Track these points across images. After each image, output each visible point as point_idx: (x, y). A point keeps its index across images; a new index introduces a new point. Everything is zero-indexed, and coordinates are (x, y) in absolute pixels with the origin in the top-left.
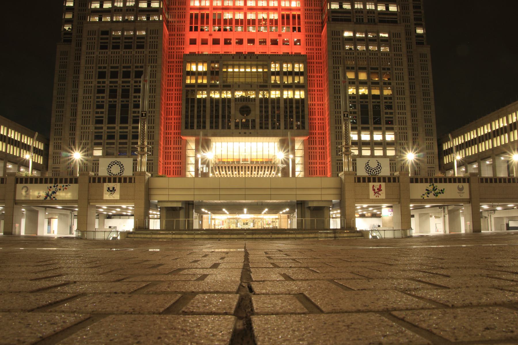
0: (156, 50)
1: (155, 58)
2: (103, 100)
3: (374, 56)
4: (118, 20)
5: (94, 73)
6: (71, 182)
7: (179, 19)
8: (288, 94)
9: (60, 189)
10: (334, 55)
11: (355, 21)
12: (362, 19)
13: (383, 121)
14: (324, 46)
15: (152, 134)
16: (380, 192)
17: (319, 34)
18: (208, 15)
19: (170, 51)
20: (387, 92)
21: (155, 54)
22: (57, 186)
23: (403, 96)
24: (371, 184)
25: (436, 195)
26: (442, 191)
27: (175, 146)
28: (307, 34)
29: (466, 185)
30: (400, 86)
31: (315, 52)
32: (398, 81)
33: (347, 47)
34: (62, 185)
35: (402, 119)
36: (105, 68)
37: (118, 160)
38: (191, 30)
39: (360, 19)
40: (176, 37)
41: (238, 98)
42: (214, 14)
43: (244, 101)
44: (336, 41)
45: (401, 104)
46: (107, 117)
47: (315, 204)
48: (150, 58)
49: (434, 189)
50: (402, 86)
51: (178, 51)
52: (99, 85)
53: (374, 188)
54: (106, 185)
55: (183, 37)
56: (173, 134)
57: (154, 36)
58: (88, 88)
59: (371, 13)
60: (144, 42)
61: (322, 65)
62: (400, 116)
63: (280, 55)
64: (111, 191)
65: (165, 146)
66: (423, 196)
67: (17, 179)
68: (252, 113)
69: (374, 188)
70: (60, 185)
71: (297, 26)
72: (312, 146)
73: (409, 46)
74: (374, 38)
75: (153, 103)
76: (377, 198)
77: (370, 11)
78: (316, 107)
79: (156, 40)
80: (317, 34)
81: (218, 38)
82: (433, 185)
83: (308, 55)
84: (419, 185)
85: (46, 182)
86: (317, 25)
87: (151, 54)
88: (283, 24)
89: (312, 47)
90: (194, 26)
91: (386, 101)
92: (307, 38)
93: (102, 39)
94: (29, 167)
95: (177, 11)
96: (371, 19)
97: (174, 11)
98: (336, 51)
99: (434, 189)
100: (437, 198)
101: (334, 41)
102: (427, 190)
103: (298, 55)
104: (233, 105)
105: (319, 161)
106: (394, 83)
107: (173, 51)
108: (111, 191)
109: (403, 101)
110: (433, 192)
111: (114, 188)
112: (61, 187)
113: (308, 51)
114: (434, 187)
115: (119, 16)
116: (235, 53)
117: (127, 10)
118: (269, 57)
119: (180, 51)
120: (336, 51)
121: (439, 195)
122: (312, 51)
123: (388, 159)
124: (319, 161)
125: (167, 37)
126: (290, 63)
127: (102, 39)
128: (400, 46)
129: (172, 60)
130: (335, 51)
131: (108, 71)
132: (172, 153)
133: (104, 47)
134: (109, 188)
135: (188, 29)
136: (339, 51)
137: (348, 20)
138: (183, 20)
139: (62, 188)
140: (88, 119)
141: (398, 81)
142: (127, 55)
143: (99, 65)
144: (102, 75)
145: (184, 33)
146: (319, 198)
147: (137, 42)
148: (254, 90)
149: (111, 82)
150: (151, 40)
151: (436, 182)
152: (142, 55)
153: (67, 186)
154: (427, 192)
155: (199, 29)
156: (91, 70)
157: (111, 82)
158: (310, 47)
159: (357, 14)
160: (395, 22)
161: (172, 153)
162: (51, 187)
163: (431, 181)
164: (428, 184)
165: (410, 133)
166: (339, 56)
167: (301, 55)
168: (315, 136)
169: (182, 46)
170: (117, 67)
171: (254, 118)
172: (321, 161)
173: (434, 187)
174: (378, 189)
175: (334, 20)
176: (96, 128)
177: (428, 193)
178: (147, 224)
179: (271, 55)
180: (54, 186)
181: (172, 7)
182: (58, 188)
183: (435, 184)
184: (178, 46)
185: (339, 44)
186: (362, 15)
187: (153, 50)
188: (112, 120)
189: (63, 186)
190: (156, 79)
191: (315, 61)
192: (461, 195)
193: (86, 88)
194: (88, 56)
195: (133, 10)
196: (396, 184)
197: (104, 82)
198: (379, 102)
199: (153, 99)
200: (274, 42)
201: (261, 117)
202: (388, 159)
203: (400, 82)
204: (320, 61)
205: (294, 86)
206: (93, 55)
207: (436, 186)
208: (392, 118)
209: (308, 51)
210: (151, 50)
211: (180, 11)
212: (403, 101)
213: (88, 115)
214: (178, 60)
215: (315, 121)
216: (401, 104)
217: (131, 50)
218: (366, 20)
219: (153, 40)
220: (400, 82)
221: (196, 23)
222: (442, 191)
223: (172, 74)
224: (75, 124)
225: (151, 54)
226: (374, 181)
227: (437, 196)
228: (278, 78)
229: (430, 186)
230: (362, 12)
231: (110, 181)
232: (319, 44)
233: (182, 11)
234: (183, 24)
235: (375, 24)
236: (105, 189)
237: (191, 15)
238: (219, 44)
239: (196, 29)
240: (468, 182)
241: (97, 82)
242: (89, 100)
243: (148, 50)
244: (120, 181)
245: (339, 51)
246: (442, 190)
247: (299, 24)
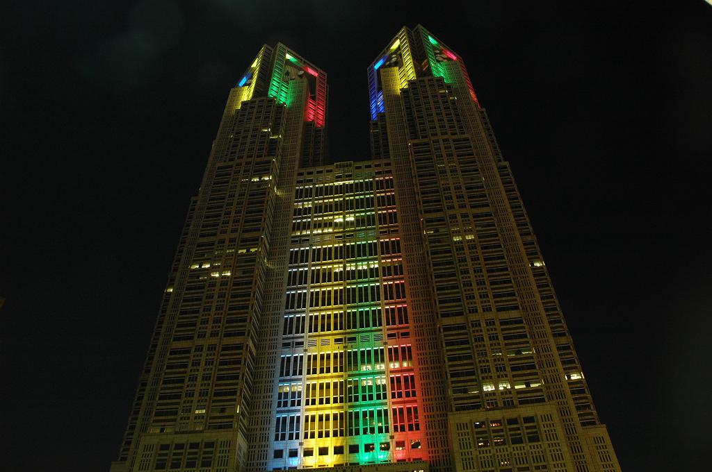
10: (464, 457)
38: (277, 439)
59: (506, 393)
60: (211, 458)
86: (440, 418)
92: (429, 437)
96: (508, 401)
101: (461, 438)
118: (377, 469)
127: (160, 455)
128: (554, 432)
135: (272, 437)
136: (469, 450)
147: (203, 458)
159: (487, 398)
166: (470, 456)
185: (468, 441)
218: (500, 404)
235: (515, 407)
237: (278, 419)
245: (469, 450)
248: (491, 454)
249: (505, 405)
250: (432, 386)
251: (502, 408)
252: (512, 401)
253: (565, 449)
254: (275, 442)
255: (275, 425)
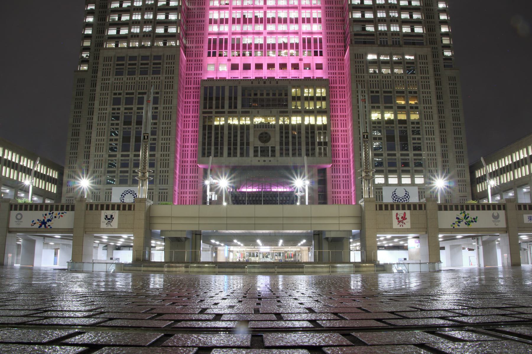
0: (172, 75)
1: (171, 84)
2: (117, 127)
3: (399, 80)
4: (134, 46)
5: (109, 100)
6: (67, 210)
7: (197, 45)
8: (309, 120)
9: (55, 217)
10: (358, 79)
11: (379, 43)
12: (387, 41)
13: (411, 147)
14: (346, 70)
15: (167, 162)
16: (404, 221)
17: (341, 58)
18: (226, 40)
19: (188, 77)
20: (415, 117)
21: (171, 80)
22: (53, 213)
23: (431, 121)
24: (394, 212)
25: (468, 224)
26: (475, 220)
27: (192, 175)
28: (329, 57)
29: (502, 213)
30: (428, 110)
31: (337, 76)
32: (425, 105)
33: (371, 71)
34: (58, 212)
35: (431, 145)
36: (120, 94)
37: (132, 188)
38: (209, 55)
39: (384, 41)
40: (193, 63)
41: (257, 125)
42: (233, 39)
43: (263, 127)
44: (359, 64)
45: (430, 129)
46: (121, 144)
47: (333, 235)
48: (167, 84)
49: (466, 217)
50: (430, 110)
51: (196, 76)
52: (114, 111)
53: (398, 216)
54: (104, 213)
55: (201, 63)
56: (189, 162)
57: (170, 61)
58: (102, 115)
59: (395, 35)
61: (345, 90)
62: (428, 141)
63: (301, 80)
64: (109, 219)
65: (181, 175)
66: (454, 225)
67: (11, 206)
68: (272, 139)
69: (398, 216)
70: (55, 213)
71: (318, 50)
72: (336, 174)
73: (436, 69)
74: (399, 61)
75: (169, 129)
76: (401, 227)
77: (395, 33)
78: (340, 133)
79: (172, 65)
80: (339, 58)
81: (236, 62)
82: (464, 212)
83: (330, 79)
84: (448, 213)
85: (41, 209)
87: (167, 80)
88: (304, 48)
89: (334, 71)
90: (212, 51)
91: (413, 126)
93: (118, 65)
94: (28, 192)
95: (195, 36)
96: (396, 41)
97: (192, 37)
98: (360, 74)
99: (466, 217)
100: (469, 227)
101: (357, 64)
102: (457, 218)
103: (320, 79)
104: (251, 131)
105: (343, 190)
106: (421, 107)
107: (190, 76)
108: (109, 219)
109: (432, 126)
110: (464, 221)
111: (112, 216)
112: (56, 214)
113: (330, 76)
114: (466, 215)
115: (136, 42)
116: (254, 78)
117: (144, 36)
118: (290, 83)
119: (198, 76)
120: (360, 74)
121: (471, 224)
122: (335, 76)
123: (416, 188)
124: (343, 190)
125: (184, 62)
126: (311, 88)
127: (118, 65)
128: (426, 69)
129: (189, 86)
130: (358, 74)
131: (123, 97)
132: (188, 182)
133: (119, 73)
134: (106, 216)
135: (206, 54)
136: (363, 75)
137: (372, 43)
138: (201, 45)
139: (58, 216)
140: (102, 146)
141: (425, 105)
142: (143, 81)
143: (114, 92)
144: (117, 101)
145: (201, 58)
146: (336, 228)
147: (153, 68)
148: (274, 116)
149: (126, 109)
150: (168, 66)
151: (467, 209)
152: (158, 80)
153: (63, 213)
154: (457, 220)
155: (217, 54)
156: (106, 97)
157: (126, 109)
158: (332, 71)
159: (381, 37)
160: (421, 44)
161: (188, 182)
162: (46, 215)
163: (462, 209)
164: (459, 212)
165: (439, 159)
166: (363, 79)
167: (323, 80)
168: (338, 164)
169: (200, 72)
170: (133, 94)
171: (274, 146)
172: (345, 190)
173: (466, 215)
174: (402, 218)
175: (356, 43)
176: (110, 156)
177: (459, 222)
178: (147, 256)
179: (291, 80)
180: (50, 214)
181: (190, 32)
182: (54, 215)
183: (467, 212)
184: (196, 72)
185: (362, 68)
186: (386, 37)
187: (170, 76)
188: (126, 148)
189: (59, 213)
190: (172, 105)
191: (338, 85)
192: (497, 223)
193: (100, 115)
194: (103, 82)
195: (150, 36)
196: (422, 212)
197: (119, 109)
198: (406, 127)
199: (169, 126)
200: (295, 66)
201: (281, 144)
202: (416, 188)
203: (428, 105)
204: (343, 85)
205: (316, 112)
206: (108, 82)
207: (468, 214)
208: (420, 143)
209: (330, 76)
210: (167, 76)
211: (198, 36)
212: (432, 126)
213: (102, 142)
214: (195, 86)
215: (339, 148)
216: (430, 129)
217: (147, 76)
218: (390, 43)
219: (170, 66)
220: (428, 105)
221: (215, 48)
222: (475, 220)
223: (189, 100)
224: (89, 152)
225: (167, 80)
226: (398, 209)
227: (469, 224)
228: (299, 103)
229: (461, 214)
230: (386, 34)
231: (108, 209)
232: (342, 68)
233: (200, 36)
234: (201, 49)
235: (401, 46)
236: (103, 217)
237: (210, 40)
238: (238, 69)
239: (214, 54)
240: (504, 209)
241: (111, 109)
242: (104, 127)
243: (165, 76)
244: (119, 209)
245: (363, 75)
246: (474, 219)
247: (321, 47)
248: (378, 79)
249: (393, 44)
250: (335, 23)
251: (391, 46)
252: (399, 41)
253: (432, 82)
254: (208, 58)
255: (207, 45)
